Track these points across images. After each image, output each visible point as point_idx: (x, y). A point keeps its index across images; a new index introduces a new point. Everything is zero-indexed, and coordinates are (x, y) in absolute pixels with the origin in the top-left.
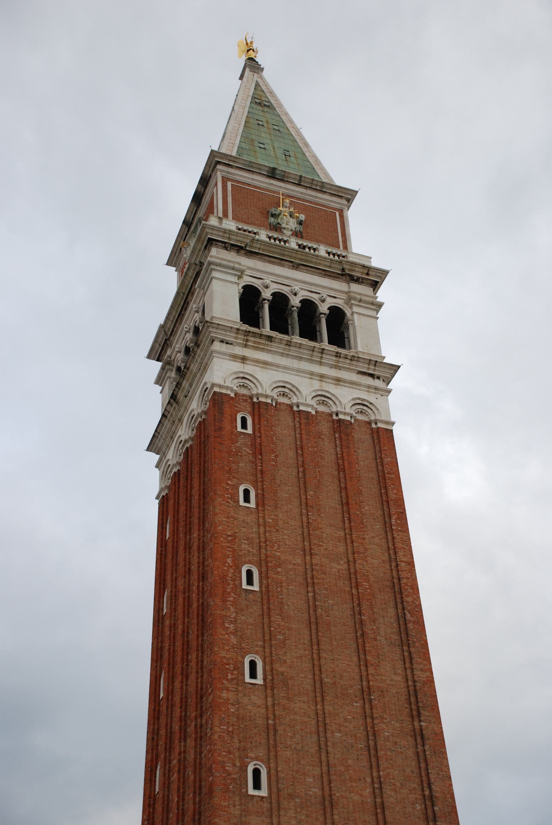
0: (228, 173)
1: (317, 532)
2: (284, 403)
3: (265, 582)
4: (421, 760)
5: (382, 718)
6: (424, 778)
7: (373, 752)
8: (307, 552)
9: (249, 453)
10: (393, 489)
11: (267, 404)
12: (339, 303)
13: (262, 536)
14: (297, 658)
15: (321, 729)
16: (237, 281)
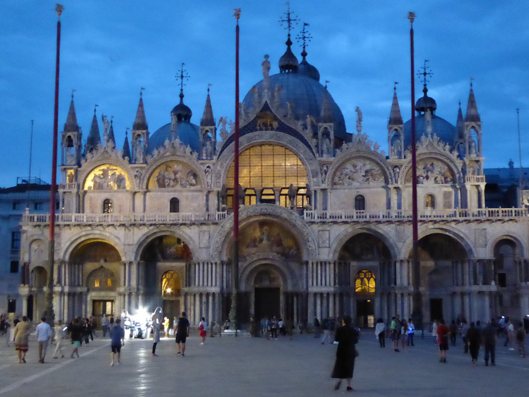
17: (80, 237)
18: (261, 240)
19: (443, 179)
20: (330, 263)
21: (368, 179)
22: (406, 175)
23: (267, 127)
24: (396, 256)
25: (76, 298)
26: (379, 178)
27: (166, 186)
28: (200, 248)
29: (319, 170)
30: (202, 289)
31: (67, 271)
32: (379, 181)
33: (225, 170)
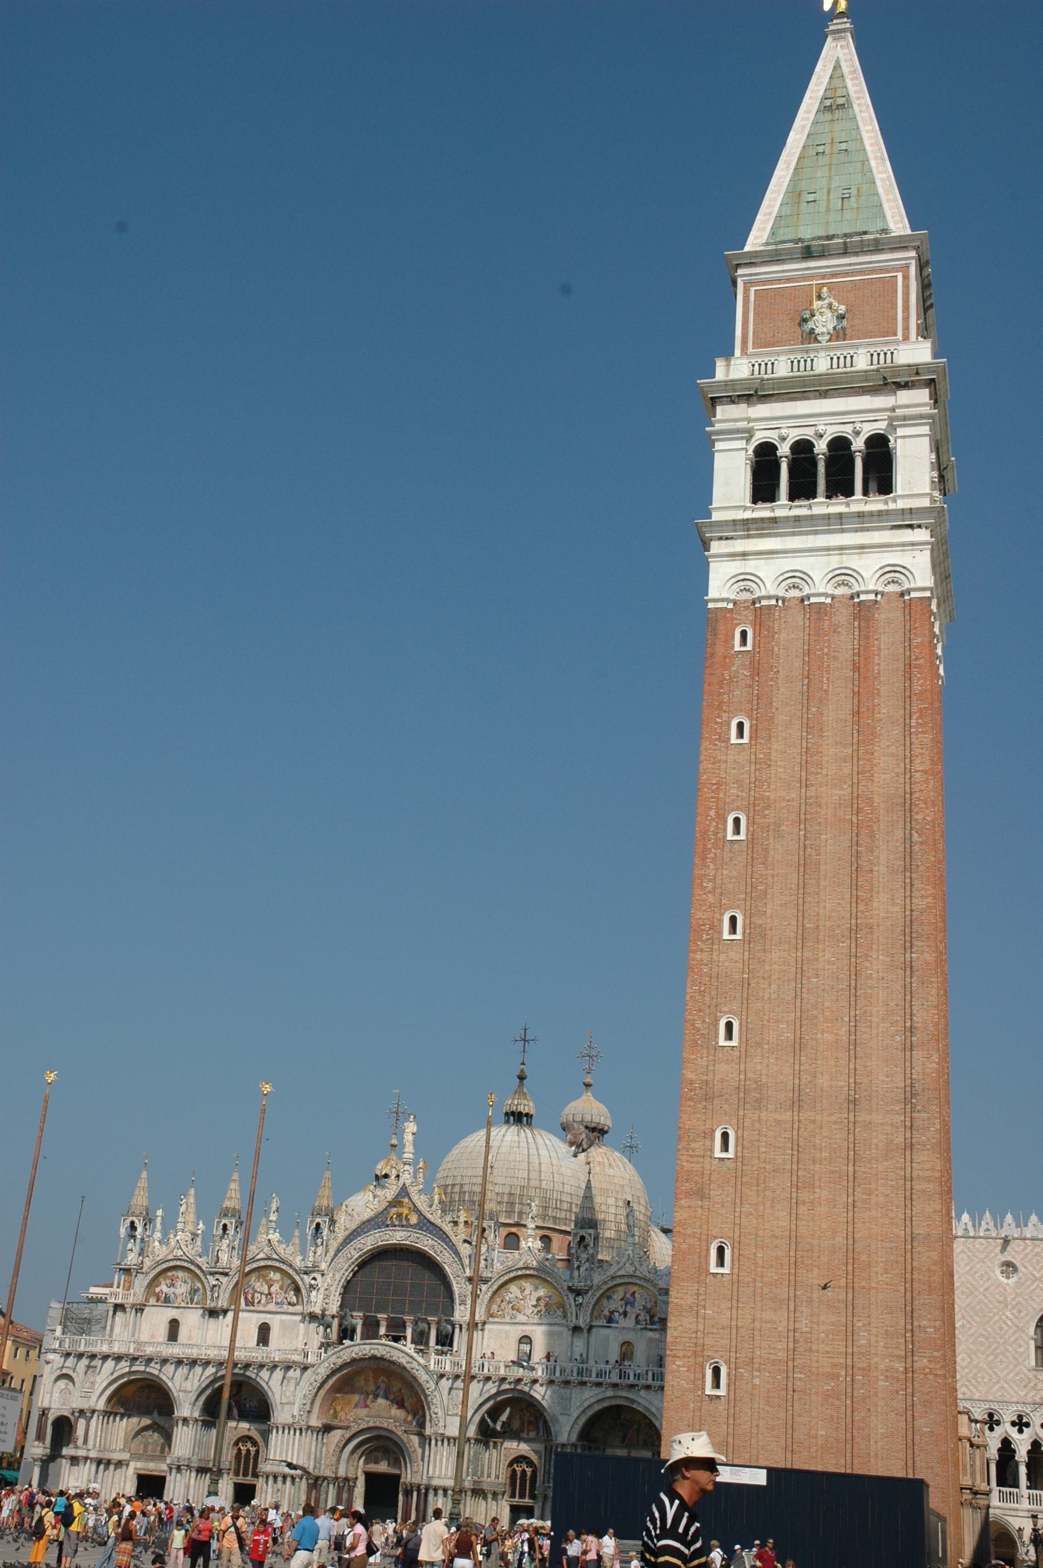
0: (751, 275)
1: (815, 758)
2: (794, 598)
3: (751, 829)
4: (908, 993)
5: (866, 956)
6: (908, 1011)
7: (853, 991)
8: (804, 784)
9: (746, 676)
10: (919, 679)
11: (769, 607)
12: (880, 427)
13: (753, 775)
14: (781, 905)
15: (799, 976)
16: (744, 446)
19: (648, 1318)
22: (593, 1309)
23: (403, 1223)
24: (556, 1437)
25: (112, 1467)
26: (556, 1311)
27: (255, 1304)
31: (100, 1427)
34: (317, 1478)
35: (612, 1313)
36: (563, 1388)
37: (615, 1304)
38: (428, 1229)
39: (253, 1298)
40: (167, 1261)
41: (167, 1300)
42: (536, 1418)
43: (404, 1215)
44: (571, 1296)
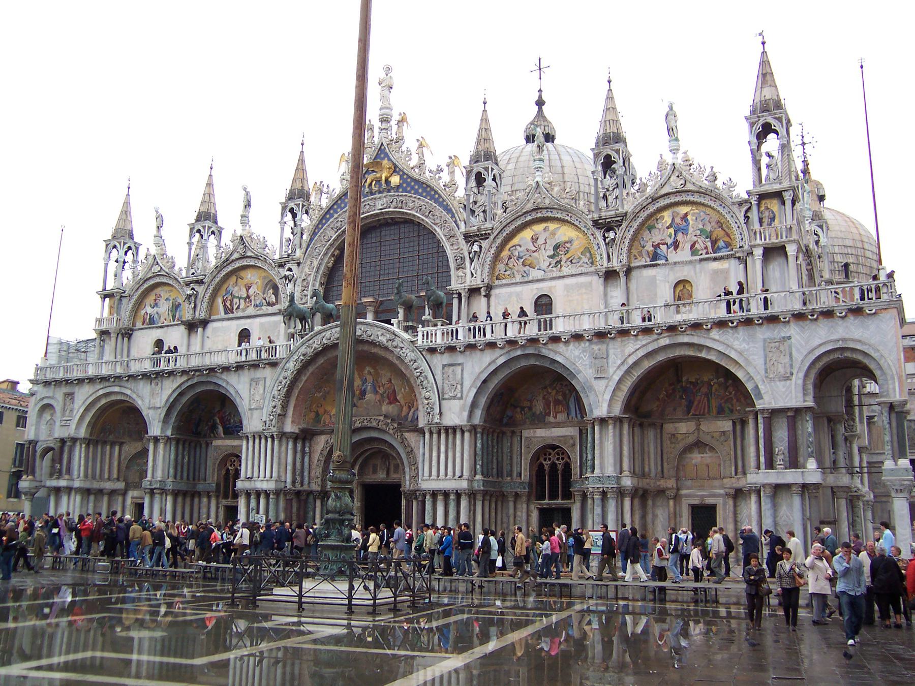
17: (98, 399)
18: (363, 393)
19: (709, 244)
20: (463, 432)
21: (560, 262)
22: (631, 246)
24: (591, 411)
25: (106, 499)
26: (580, 258)
27: (234, 311)
28: (250, 409)
29: (466, 254)
30: (248, 485)
31: (83, 455)
32: (581, 262)
33: (317, 272)
34: (298, 493)
35: (656, 247)
36: (596, 343)
37: (662, 232)
38: (412, 188)
39: (231, 304)
40: (147, 280)
41: (152, 321)
42: (564, 395)
43: (383, 178)
44: (599, 234)
